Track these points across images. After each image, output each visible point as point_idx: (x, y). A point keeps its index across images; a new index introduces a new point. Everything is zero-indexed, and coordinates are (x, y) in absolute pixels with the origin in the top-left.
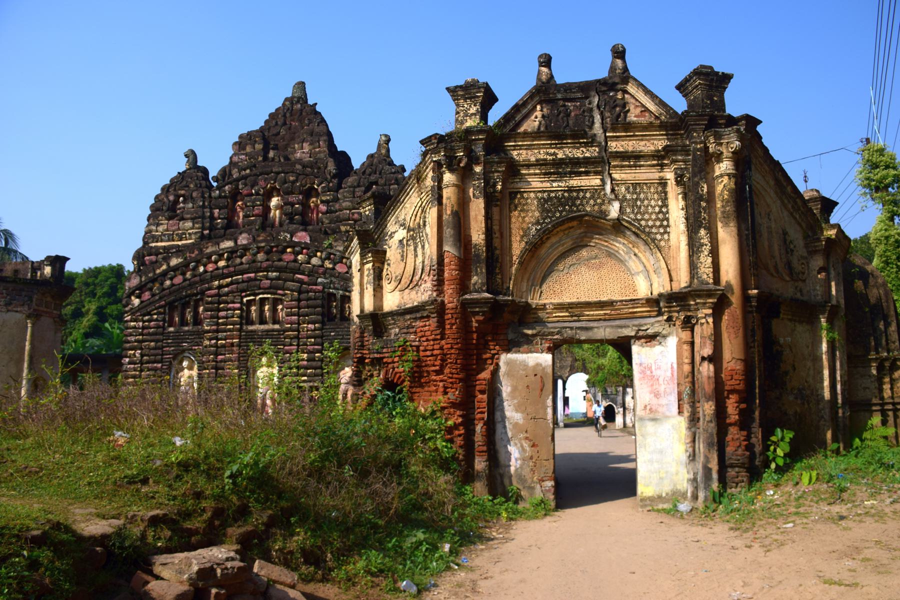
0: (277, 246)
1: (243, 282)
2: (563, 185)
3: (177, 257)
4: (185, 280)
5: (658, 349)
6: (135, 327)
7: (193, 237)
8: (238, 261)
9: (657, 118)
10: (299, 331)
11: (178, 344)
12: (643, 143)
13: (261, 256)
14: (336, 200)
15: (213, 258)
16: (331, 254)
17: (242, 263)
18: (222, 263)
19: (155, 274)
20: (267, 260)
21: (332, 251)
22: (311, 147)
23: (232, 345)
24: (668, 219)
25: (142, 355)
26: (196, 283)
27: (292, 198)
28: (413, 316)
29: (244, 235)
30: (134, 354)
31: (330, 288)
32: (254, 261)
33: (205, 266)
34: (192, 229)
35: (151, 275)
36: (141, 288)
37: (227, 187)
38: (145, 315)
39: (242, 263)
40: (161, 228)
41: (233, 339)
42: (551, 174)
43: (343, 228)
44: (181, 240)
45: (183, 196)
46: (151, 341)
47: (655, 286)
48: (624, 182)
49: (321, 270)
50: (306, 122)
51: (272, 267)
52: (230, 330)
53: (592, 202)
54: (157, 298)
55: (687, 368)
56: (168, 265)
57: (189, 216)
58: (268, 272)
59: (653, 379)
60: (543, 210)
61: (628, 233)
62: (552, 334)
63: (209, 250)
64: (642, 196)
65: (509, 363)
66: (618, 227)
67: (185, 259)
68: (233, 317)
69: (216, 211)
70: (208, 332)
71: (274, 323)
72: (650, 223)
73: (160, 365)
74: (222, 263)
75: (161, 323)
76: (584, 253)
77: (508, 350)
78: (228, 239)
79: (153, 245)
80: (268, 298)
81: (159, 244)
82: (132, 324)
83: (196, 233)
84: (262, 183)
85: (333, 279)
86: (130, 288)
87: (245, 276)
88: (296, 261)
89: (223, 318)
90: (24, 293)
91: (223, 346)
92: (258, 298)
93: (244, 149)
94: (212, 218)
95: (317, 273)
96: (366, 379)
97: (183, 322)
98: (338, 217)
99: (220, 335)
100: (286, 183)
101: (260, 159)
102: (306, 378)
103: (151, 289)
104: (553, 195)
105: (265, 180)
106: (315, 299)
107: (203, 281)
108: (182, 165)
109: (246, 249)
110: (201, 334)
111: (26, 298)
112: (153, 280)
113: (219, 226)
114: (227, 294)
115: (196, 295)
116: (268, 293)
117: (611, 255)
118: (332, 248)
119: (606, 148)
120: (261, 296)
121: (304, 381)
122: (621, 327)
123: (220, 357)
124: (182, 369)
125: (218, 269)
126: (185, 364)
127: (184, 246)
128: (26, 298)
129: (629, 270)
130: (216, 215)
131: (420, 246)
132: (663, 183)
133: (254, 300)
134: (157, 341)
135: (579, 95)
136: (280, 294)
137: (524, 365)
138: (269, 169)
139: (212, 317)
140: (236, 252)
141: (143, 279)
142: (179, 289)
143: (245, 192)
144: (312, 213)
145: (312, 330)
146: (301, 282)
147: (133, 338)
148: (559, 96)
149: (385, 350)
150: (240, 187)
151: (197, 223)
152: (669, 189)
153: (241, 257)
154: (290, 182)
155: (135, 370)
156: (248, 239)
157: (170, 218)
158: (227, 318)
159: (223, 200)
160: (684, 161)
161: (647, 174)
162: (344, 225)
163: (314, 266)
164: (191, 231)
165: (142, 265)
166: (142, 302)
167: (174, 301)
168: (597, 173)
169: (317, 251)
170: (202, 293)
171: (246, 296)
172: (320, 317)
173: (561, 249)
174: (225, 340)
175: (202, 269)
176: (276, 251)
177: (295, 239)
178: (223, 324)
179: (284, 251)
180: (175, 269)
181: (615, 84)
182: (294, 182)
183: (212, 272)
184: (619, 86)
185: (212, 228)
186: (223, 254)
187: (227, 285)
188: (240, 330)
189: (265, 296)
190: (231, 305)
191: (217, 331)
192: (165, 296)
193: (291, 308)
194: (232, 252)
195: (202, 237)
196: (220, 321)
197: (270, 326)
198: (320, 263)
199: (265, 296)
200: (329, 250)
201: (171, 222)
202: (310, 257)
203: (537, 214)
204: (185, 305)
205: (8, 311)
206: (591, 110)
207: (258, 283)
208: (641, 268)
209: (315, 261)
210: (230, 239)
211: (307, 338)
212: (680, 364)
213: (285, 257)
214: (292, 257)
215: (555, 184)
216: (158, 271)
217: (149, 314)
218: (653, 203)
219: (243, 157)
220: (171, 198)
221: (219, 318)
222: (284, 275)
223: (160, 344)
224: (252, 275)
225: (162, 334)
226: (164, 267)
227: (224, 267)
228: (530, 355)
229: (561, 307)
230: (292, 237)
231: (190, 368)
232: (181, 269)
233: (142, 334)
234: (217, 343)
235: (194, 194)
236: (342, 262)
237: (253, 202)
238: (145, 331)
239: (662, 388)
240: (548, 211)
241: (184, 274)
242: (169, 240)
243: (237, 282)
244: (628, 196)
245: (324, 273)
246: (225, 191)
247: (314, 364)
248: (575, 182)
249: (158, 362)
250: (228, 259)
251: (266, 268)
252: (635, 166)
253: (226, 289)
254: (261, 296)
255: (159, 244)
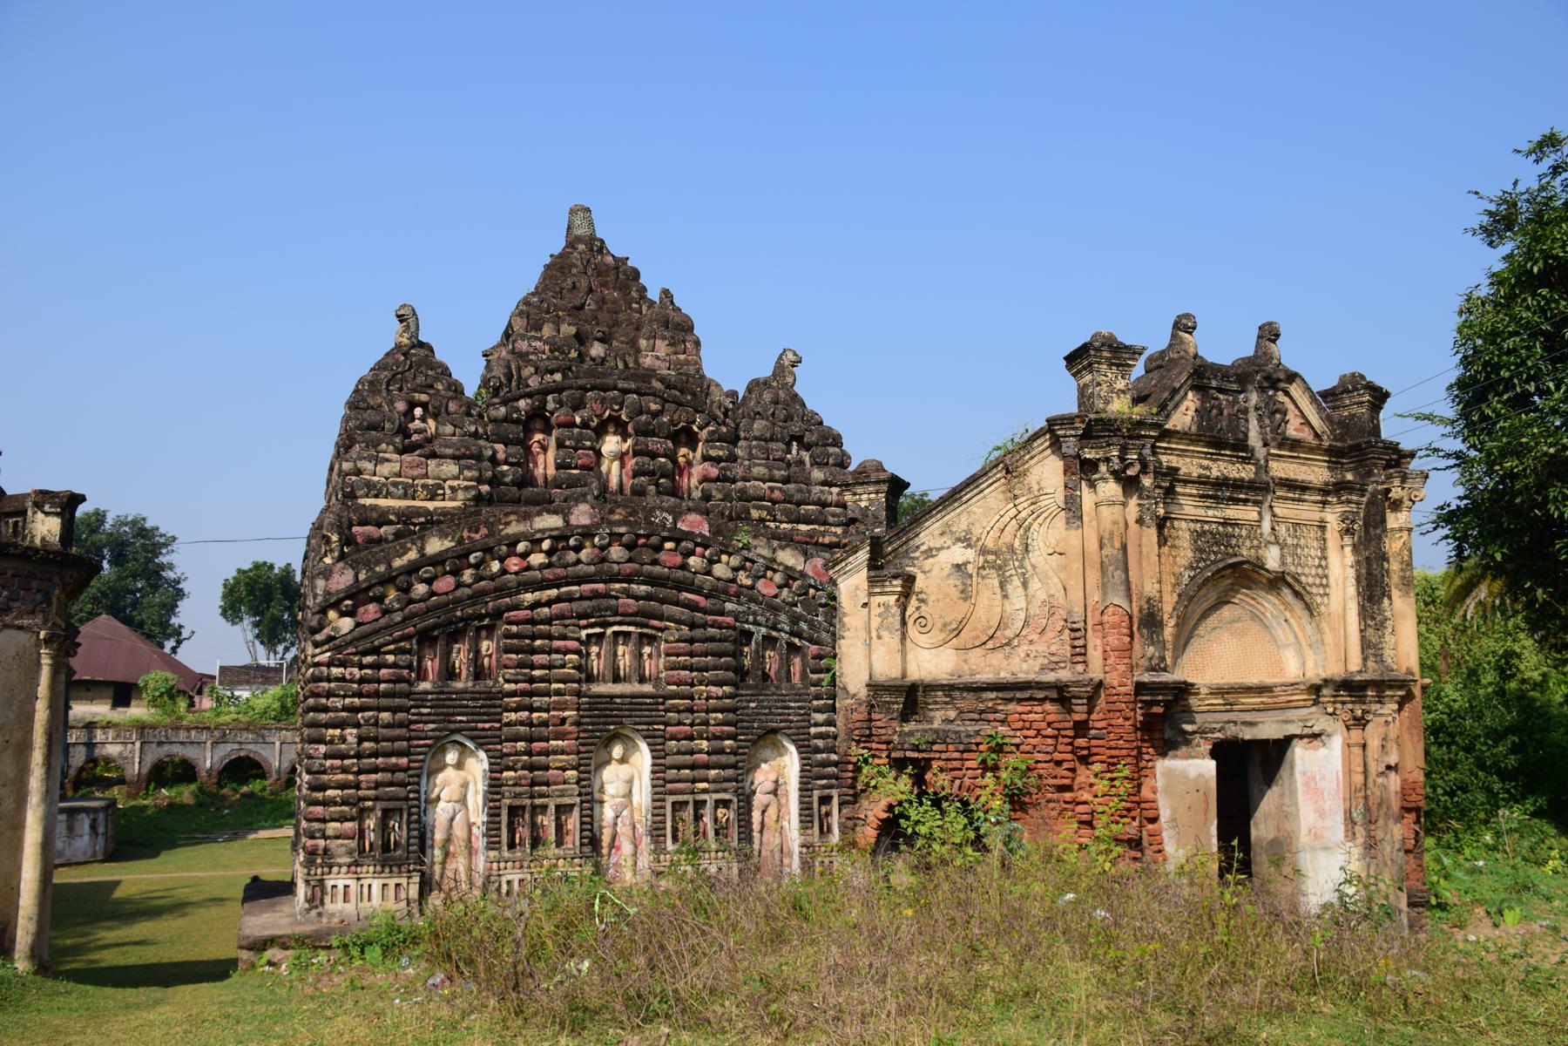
0: (647, 537)
1: (582, 598)
2: (1218, 514)
3: (443, 536)
4: (459, 585)
5: (1322, 752)
6: (343, 679)
7: (461, 495)
8: (571, 556)
9: (1317, 435)
10: (692, 698)
11: (447, 718)
12: (1304, 468)
13: (616, 552)
14: (733, 458)
15: (521, 547)
16: (747, 559)
17: (579, 562)
18: (537, 559)
19: (389, 566)
20: (630, 560)
21: (750, 555)
22: (671, 349)
23: (563, 721)
24: (1326, 577)
25: (361, 740)
26: (483, 593)
27: (655, 444)
28: (1000, 695)
29: (583, 507)
30: (343, 739)
31: (747, 622)
32: (604, 560)
33: (502, 560)
34: (457, 478)
35: (381, 569)
36: (358, 595)
37: (522, 403)
38: (365, 653)
39: (579, 562)
40: (385, 469)
41: (563, 710)
42: (1208, 497)
43: (755, 514)
44: (431, 499)
45: (424, 406)
46: (380, 709)
47: (1310, 664)
48: (1285, 520)
49: (733, 588)
50: (634, 294)
51: (638, 573)
52: (558, 693)
53: (1248, 543)
54: (398, 617)
55: (1359, 779)
56: (421, 550)
57: (449, 451)
58: (630, 582)
59: (1316, 793)
60: (1199, 550)
61: (1286, 591)
62: (1212, 731)
63: (514, 528)
64: (1302, 542)
65: (1169, 773)
66: (1277, 582)
67: (460, 542)
68: (563, 666)
69: (500, 447)
70: (513, 694)
71: (642, 680)
72: (1311, 580)
73: (404, 761)
74: (537, 559)
75: (405, 672)
76: (1226, 611)
77: (1163, 755)
78: (549, 512)
79: (368, 502)
80: (627, 635)
81: (382, 502)
82: (336, 671)
83: (467, 488)
84: (597, 407)
85: (752, 605)
86: (327, 593)
87: (586, 587)
88: (684, 567)
89: (542, 667)
90: (35, 584)
91: (545, 724)
92: (609, 631)
93: (539, 329)
94: (493, 460)
95: (726, 592)
96: (863, 791)
97: (450, 673)
98: (743, 491)
99: (537, 701)
100: (641, 413)
101: (574, 354)
102: (705, 785)
103: (379, 600)
104: (1206, 527)
105: (603, 401)
106: (720, 640)
107: (502, 591)
108: (386, 337)
109: (587, 533)
110: (492, 702)
111: (39, 597)
112: (388, 580)
113: (508, 479)
114: (548, 621)
115: (481, 617)
116: (629, 624)
117: (1255, 617)
118: (749, 550)
119: (1267, 470)
120: (616, 628)
121: (705, 791)
122: (1286, 722)
123: (537, 746)
124: (444, 767)
125: (529, 568)
126: (451, 757)
127: (444, 513)
128: (39, 597)
129: (1275, 640)
130: (501, 456)
131: (1016, 582)
132: (1322, 527)
133: (602, 635)
134: (394, 710)
135: (1235, 387)
136: (653, 628)
137: (1184, 776)
138: (609, 381)
139: (521, 665)
140: (567, 538)
141: (362, 577)
142: (446, 604)
143: (560, 416)
144: (681, 475)
145: (718, 698)
146: (693, 607)
147: (339, 703)
148: (1214, 383)
149: (935, 747)
150: (551, 406)
151: (469, 468)
152: (1328, 535)
153: (577, 549)
154: (649, 412)
155: (345, 770)
156: (592, 516)
157: (401, 452)
158: (550, 667)
159: (513, 428)
160: (1358, 503)
161: (1307, 511)
162: (759, 508)
163: (718, 579)
164: (455, 483)
165: (348, 544)
166: (358, 625)
167: (435, 627)
168: (1256, 503)
169: (722, 552)
170: (497, 614)
171: (585, 627)
172: (731, 674)
173: (1205, 605)
174: (547, 711)
175: (495, 566)
176: (644, 545)
177: (681, 526)
178: (541, 680)
179: (659, 548)
180: (437, 560)
181: (1279, 380)
182: (655, 415)
183: (516, 573)
184: (1282, 385)
185: (495, 481)
186: (541, 540)
187: (549, 603)
188: (578, 694)
189: (625, 628)
190: (557, 644)
191: (531, 694)
192: (415, 615)
193: (678, 655)
194: (560, 538)
195: (479, 498)
196: (537, 673)
197: (636, 687)
198: (729, 575)
199: (625, 628)
200: (745, 553)
201: (407, 457)
202: (711, 562)
203: (1190, 554)
204: (456, 636)
205: (6, 626)
206: (1246, 411)
207: (613, 602)
208: (1292, 639)
209: (720, 570)
210: (555, 512)
211: (707, 712)
212: (1349, 772)
213: (662, 556)
214: (678, 559)
215: (1210, 513)
216: (397, 563)
217: (376, 651)
218: (1313, 553)
219: (538, 344)
220: (401, 406)
221: (533, 667)
222: (663, 592)
223: (401, 716)
224: (600, 587)
225: (408, 695)
226: (413, 555)
227: (542, 567)
228: (1190, 761)
229: (1219, 691)
230: (675, 523)
231: (459, 766)
232: (454, 562)
233: (359, 695)
234: (529, 718)
235: (452, 407)
236: (764, 576)
237: (578, 441)
238: (367, 687)
239: (1327, 805)
240: (1201, 551)
241: (456, 572)
242: (405, 496)
243: (569, 598)
244: (1289, 541)
245: (737, 595)
246: (518, 410)
247: (723, 759)
248: (1232, 512)
249: (400, 754)
250: (549, 553)
251: (630, 575)
252: (1299, 500)
253: (546, 610)
254: (616, 628)
255: (382, 502)
